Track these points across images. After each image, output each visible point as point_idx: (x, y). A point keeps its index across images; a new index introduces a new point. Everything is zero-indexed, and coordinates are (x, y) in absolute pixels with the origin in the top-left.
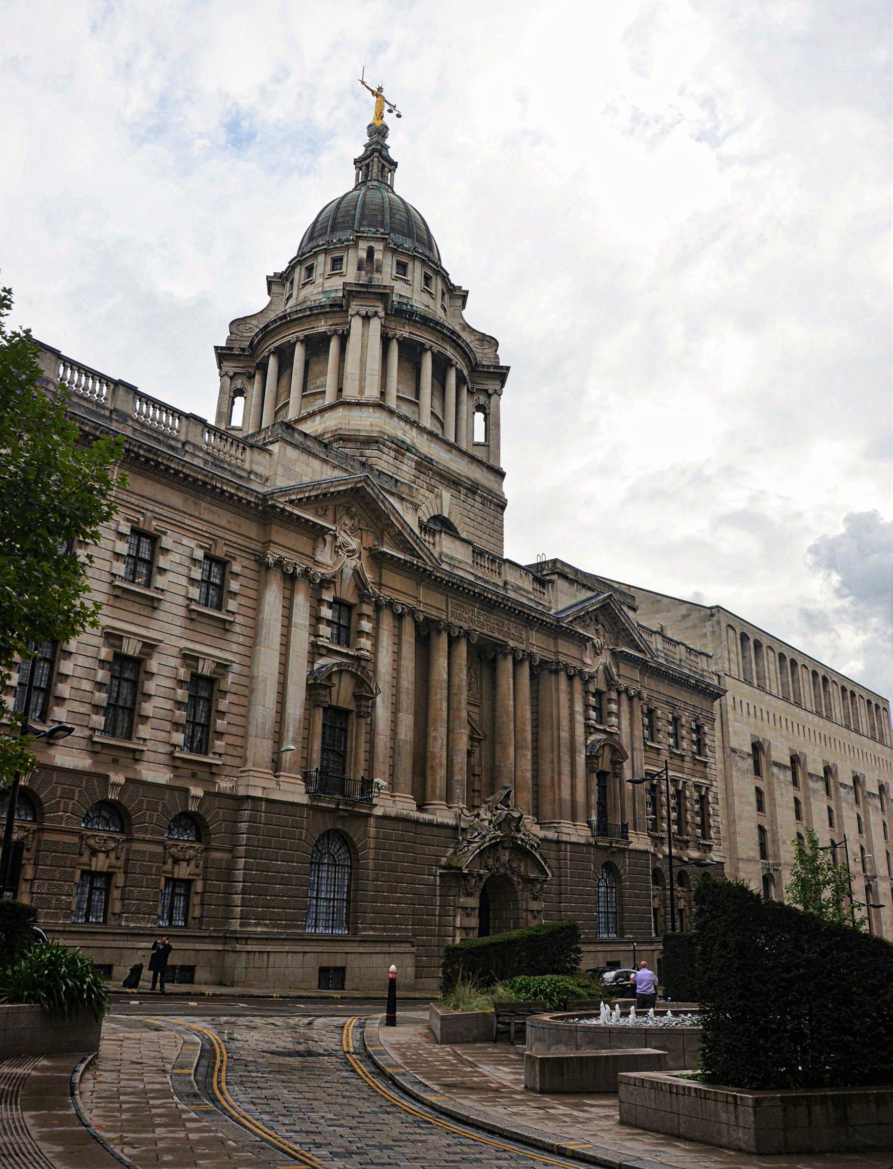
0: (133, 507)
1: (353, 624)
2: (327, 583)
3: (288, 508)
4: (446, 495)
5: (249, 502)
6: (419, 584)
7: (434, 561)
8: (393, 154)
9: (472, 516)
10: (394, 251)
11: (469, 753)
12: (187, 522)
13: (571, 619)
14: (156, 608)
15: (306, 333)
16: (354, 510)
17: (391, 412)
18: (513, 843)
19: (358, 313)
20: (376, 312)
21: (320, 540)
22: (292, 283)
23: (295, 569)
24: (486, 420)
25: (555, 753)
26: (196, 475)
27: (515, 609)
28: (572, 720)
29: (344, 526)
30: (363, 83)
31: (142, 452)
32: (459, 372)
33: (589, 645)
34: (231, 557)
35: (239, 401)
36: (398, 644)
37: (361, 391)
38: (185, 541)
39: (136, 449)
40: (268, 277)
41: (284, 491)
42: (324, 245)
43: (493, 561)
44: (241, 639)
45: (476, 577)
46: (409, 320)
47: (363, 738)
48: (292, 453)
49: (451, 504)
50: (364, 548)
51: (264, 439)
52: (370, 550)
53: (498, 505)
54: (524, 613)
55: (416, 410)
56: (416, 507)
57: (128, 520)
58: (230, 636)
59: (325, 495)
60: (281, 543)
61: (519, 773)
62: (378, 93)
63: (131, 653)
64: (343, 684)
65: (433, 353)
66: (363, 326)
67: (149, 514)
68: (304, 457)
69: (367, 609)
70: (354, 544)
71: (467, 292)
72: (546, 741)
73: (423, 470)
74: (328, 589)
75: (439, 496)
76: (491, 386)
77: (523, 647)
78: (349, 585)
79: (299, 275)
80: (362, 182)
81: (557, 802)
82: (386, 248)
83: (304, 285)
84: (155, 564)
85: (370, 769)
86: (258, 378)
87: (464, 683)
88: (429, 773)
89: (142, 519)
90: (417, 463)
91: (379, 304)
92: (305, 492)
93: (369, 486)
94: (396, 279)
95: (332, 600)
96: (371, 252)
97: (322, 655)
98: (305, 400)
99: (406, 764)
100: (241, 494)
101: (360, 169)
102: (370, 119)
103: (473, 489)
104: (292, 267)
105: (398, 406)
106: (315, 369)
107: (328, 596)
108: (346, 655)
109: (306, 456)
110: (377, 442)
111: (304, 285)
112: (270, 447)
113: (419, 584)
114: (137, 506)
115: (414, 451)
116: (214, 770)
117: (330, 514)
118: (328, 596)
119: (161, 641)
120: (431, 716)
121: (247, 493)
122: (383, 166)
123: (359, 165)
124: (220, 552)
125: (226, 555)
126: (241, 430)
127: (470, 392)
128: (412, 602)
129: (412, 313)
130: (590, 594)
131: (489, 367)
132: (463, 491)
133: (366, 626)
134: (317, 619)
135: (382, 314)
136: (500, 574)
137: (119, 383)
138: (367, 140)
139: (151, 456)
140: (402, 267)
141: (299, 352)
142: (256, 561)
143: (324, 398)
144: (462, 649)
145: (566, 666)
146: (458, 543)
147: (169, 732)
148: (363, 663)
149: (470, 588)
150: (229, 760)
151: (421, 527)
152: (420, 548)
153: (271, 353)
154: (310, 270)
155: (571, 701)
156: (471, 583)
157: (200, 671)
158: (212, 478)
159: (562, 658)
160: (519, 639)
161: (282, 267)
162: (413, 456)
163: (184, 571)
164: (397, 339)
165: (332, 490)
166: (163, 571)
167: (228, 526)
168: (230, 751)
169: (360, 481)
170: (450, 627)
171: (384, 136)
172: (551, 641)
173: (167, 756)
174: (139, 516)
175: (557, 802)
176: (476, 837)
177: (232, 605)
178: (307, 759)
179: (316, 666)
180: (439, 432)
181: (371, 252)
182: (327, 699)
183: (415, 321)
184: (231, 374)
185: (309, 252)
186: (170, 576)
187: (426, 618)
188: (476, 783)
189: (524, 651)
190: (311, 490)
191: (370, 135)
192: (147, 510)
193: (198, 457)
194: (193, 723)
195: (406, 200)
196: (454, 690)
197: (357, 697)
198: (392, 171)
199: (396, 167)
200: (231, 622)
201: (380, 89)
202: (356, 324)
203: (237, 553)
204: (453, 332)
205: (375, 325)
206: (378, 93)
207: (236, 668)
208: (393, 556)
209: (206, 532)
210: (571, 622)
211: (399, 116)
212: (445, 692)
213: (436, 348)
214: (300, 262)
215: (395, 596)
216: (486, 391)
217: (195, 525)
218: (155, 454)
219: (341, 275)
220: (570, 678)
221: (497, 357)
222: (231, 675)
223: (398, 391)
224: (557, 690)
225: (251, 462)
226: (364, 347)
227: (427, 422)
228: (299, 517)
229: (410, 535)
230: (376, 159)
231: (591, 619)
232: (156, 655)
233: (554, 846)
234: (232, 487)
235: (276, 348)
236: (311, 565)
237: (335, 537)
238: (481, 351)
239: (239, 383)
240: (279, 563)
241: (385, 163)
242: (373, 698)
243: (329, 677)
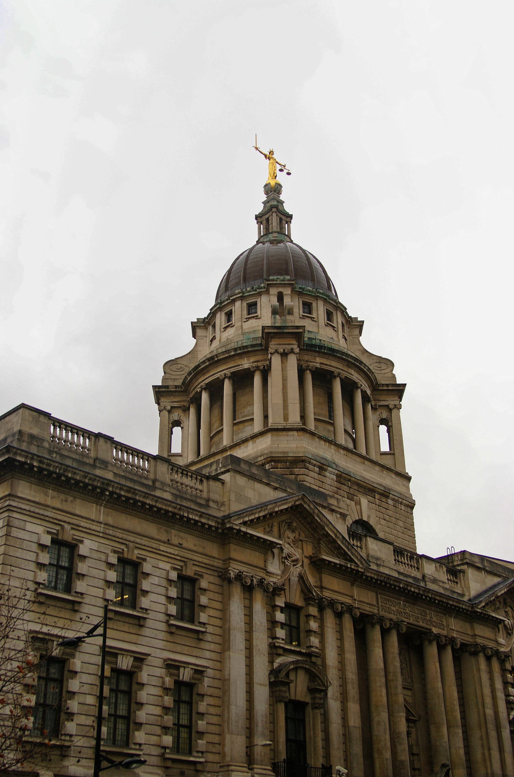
0: (117, 540)
1: (302, 625)
2: (278, 590)
3: (243, 529)
4: (364, 501)
5: (210, 526)
6: (353, 585)
7: (364, 562)
8: (288, 208)
9: (387, 518)
10: (300, 293)
11: (409, 733)
12: (162, 548)
13: (483, 604)
14: (142, 626)
15: (232, 370)
16: (294, 524)
17: (313, 434)
19: (276, 351)
20: (292, 349)
21: (270, 553)
22: (214, 327)
23: (252, 581)
24: (388, 431)
25: (483, 730)
26: (167, 508)
27: (435, 599)
28: (494, 697)
29: (287, 540)
30: (257, 149)
31: (123, 493)
32: (364, 393)
33: (501, 626)
34: (199, 575)
35: (177, 431)
36: (341, 639)
37: (286, 418)
38: (162, 565)
39: (118, 491)
40: (192, 323)
41: (240, 514)
42: (239, 293)
43: (412, 558)
44: (212, 647)
45: (399, 573)
46: (319, 352)
47: (319, 727)
48: (241, 480)
49: (370, 509)
50: (306, 557)
51: (216, 470)
52: (310, 558)
53: (407, 506)
54: (443, 602)
55: (331, 428)
56: (343, 516)
57: (115, 552)
58: (203, 645)
59: (271, 514)
60: (239, 559)
61: (453, 750)
62: (269, 156)
63: (124, 667)
64: (299, 679)
65: (341, 380)
66: (282, 362)
67: (131, 545)
68: (251, 482)
69: (313, 611)
70: (297, 554)
71: (363, 322)
72: (474, 718)
73: (343, 481)
74: (279, 595)
75: (359, 503)
76: (391, 402)
77: (445, 633)
78: (296, 590)
79: (220, 319)
80: (263, 236)
82: (293, 291)
83: (226, 328)
84: (139, 587)
85: (327, 756)
86: (192, 411)
87: (399, 670)
88: (376, 755)
89: (126, 549)
90: (338, 476)
91: (294, 342)
92: (256, 513)
93: (305, 503)
94: (304, 317)
95: (283, 606)
96: (280, 297)
97: (279, 655)
98: (235, 428)
99: (357, 748)
100: (203, 521)
101: (261, 223)
102: (265, 179)
103: (385, 494)
104: (213, 313)
105: (316, 427)
106: (242, 400)
107: (280, 602)
108: (299, 653)
109: (253, 482)
110: (303, 461)
111: (226, 328)
112: (222, 477)
113: (353, 585)
114: (122, 539)
115: (334, 466)
116: (199, 767)
117: (275, 529)
118: (280, 602)
119: (149, 655)
120: (373, 703)
121: (209, 519)
122: (281, 220)
123: (260, 220)
124: (190, 572)
125: (195, 574)
126: (181, 456)
127: (374, 409)
128: (348, 600)
129: (321, 347)
130: (496, 580)
131: (387, 385)
132: (377, 496)
133: (314, 625)
134: (273, 623)
135: (297, 350)
136: (418, 568)
137: (99, 436)
138: (264, 198)
139: (130, 495)
140: (308, 307)
141: (227, 387)
142: (219, 576)
143: (252, 425)
144: (394, 639)
145: (484, 648)
146: (379, 543)
147: (160, 736)
148: (314, 659)
149: (396, 583)
150: (211, 757)
151: (349, 534)
152: (352, 553)
153: (202, 389)
154: (229, 315)
155: (492, 679)
156: (397, 580)
157: (181, 678)
158: (180, 509)
159: (479, 641)
160: (440, 626)
161: (204, 313)
162: (334, 471)
163: (163, 591)
165: (276, 509)
166: (145, 593)
167: (195, 549)
168: (211, 748)
169: (298, 499)
170: (382, 620)
171: (279, 193)
172: (468, 626)
173: (159, 758)
174: (123, 547)
177: (203, 617)
178: (274, 751)
179: (276, 665)
180: (351, 446)
181: (280, 297)
182: (287, 694)
183: (324, 353)
184: (169, 408)
185: (227, 300)
186: (152, 597)
187: (361, 614)
188: (416, 762)
189: (446, 637)
190: (260, 512)
191: (267, 193)
192: (130, 541)
193: (166, 491)
194: (178, 725)
195: (304, 248)
196: (390, 677)
197: (311, 691)
198: (289, 222)
199: (292, 219)
200: (203, 632)
201: (271, 152)
202: (276, 361)
203: (204, 570)
204: (356, 359)
205: (292, 361)
206: (269, 156)
207: (210, 672)
208: (330, 562)
209: (177, 555)
210: (484, 607)
211: (289, 174)
212: (383, 680)
213: (344, 374)
214: (220, 309)
215: (335, 596)
216: (387, 406)
217: (169, 550)
218: (133, 493)
219: (257, 318)
220: (488, 659)
221: (394, 376)
222: (206, 679)
223: (315, 414)
224: (479, 670)
225: (209, 492)
226: (284, 380)
227: (342, 439)
228: (252, 536)
229: (343, 543)
230: (274, 214)
231: (500, 602)
232: (145, 667)
234: (197, 515)
235: (207, 384)
236: (264, 575)
237: (282, 550)
238: (380, 372)
239: (175, 416)
240: (239, 577)
241: (283, 217)
242: (325, 692)
243: (287, 675)
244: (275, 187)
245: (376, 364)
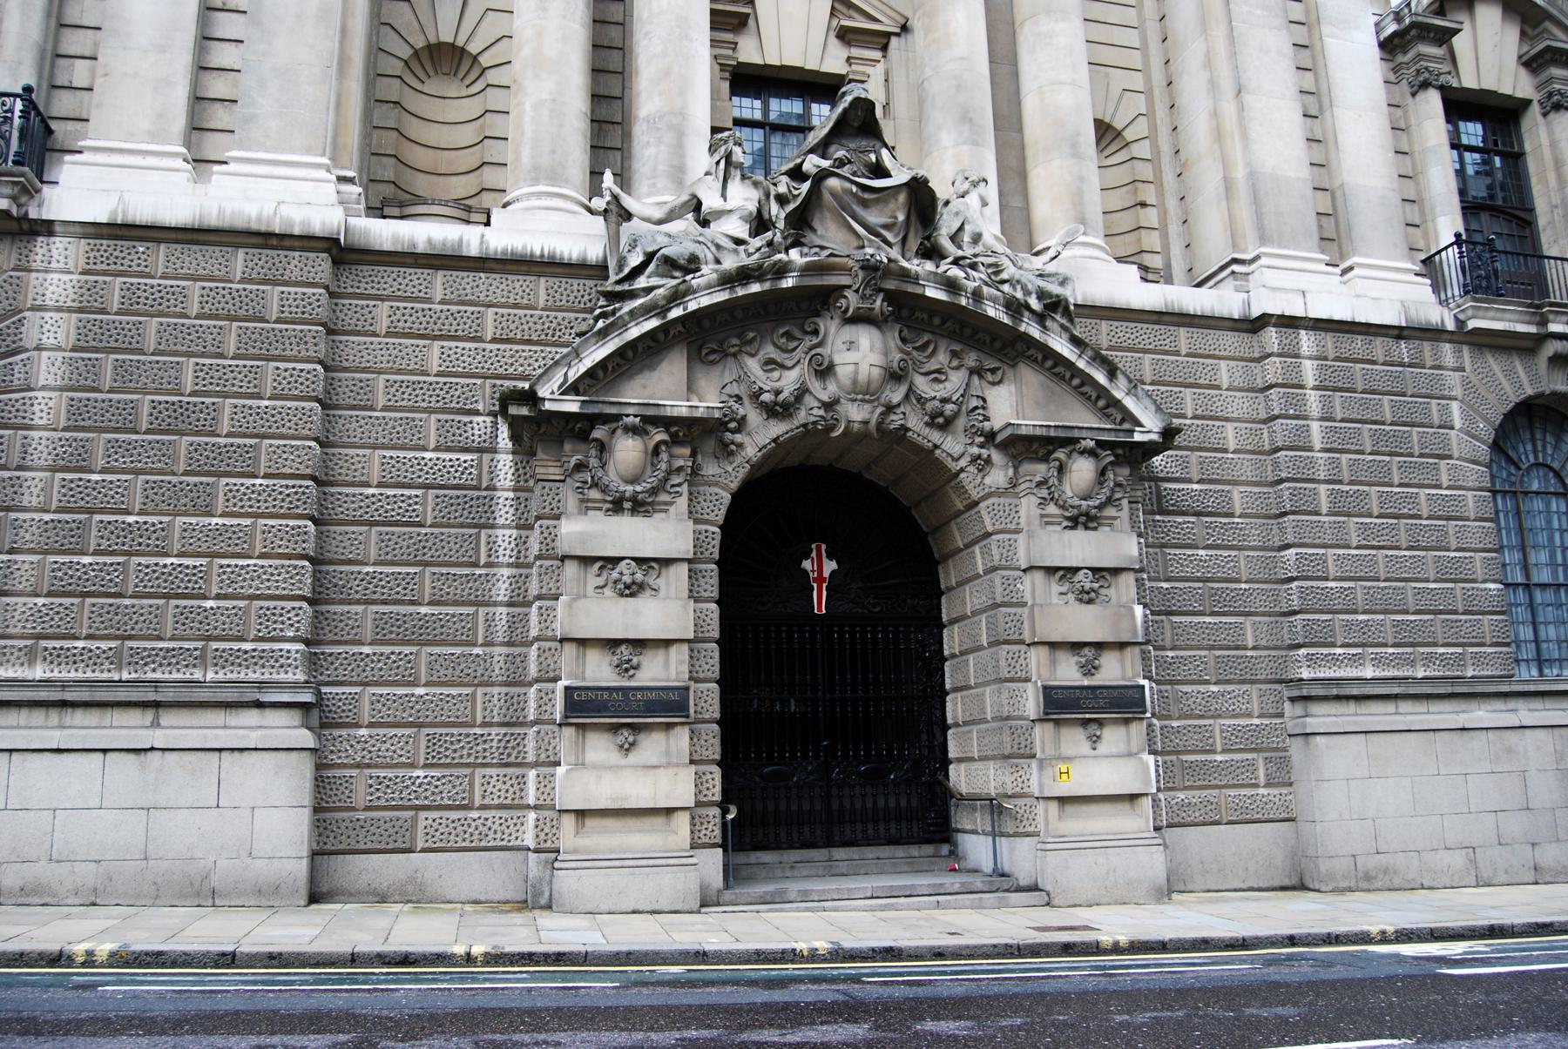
18: (890, 297)
25: (1219, 32)
81: (1242, 189)
175: (1242, 189)
176: (638, 271)
233: (1229, 341)
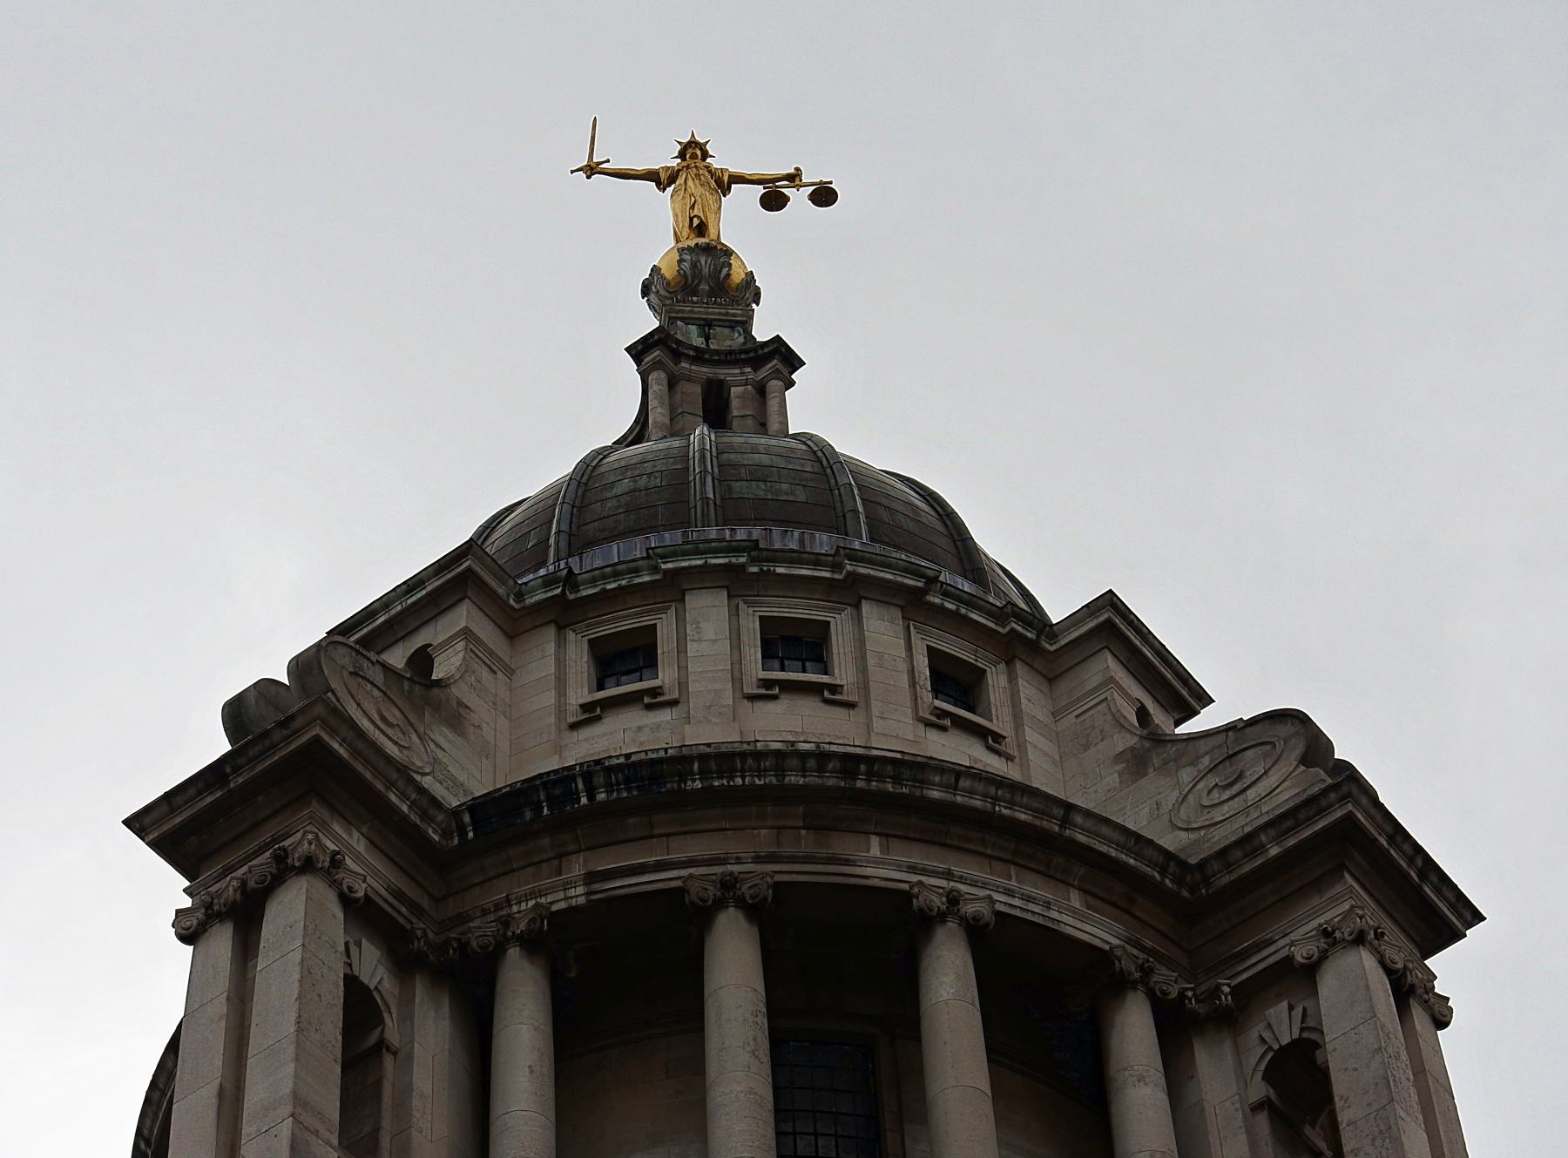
20: (281, 858)
164: (532, 944)
201: (693, 151)
211: (824, 196)
238: (1237, 804)
244: (681, 274)
245: (1212, 780)
